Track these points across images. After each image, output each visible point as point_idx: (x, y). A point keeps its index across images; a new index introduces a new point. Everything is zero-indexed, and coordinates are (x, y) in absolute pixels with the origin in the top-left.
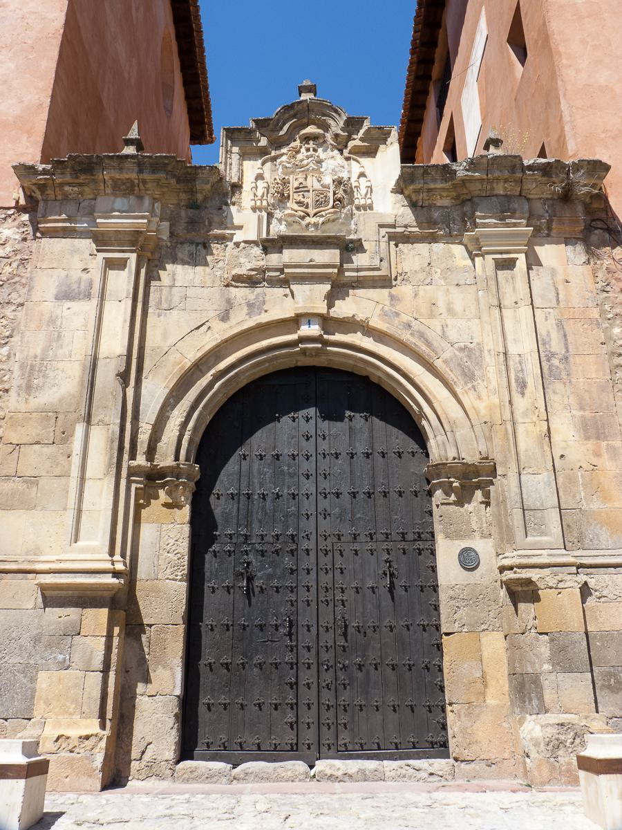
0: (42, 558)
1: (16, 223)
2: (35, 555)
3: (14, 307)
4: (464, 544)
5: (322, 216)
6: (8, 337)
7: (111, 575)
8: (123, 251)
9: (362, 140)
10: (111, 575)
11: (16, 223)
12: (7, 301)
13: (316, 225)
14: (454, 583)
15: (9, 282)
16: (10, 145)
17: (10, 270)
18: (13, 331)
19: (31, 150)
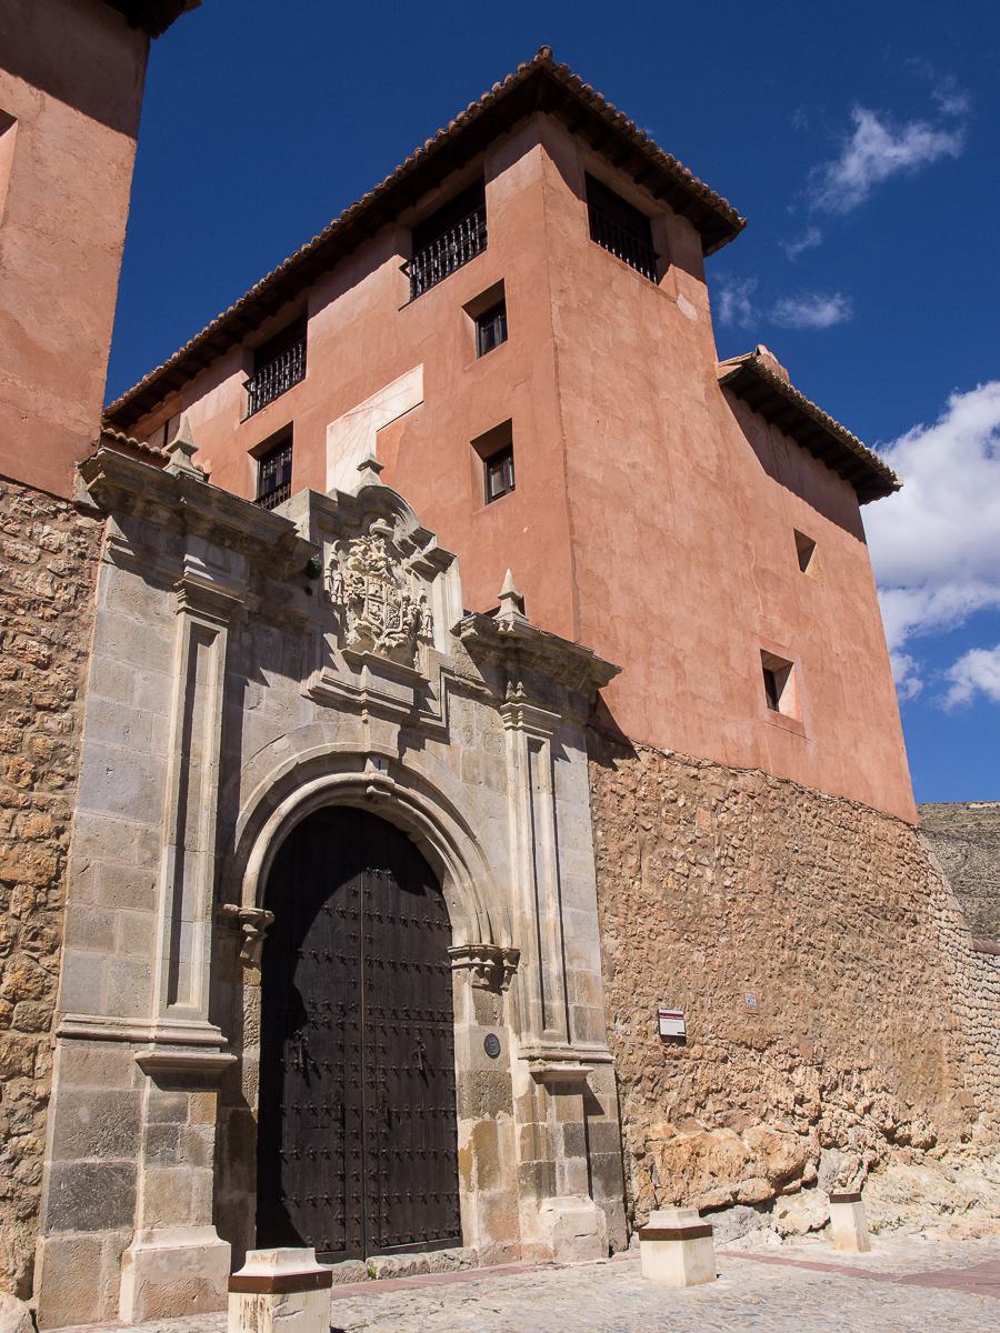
0: (130, 1021)
1: (70, 526)
2: (119, 1015)
3: (73, 656)
4: (489, 1030)
5: (394, 639)
6: (69, 699)
7: (218, 1049)
8: (213, 621)
9: (426, 557)
10: (218, 1049)
11: (70, 526)
12: (63, 642)
13: (389, 649)
14: (480, 1069)
15: (65, 614)
16: (58, 399)
17: (67, 597)
18: (75, 690)
19: (88, 421)
